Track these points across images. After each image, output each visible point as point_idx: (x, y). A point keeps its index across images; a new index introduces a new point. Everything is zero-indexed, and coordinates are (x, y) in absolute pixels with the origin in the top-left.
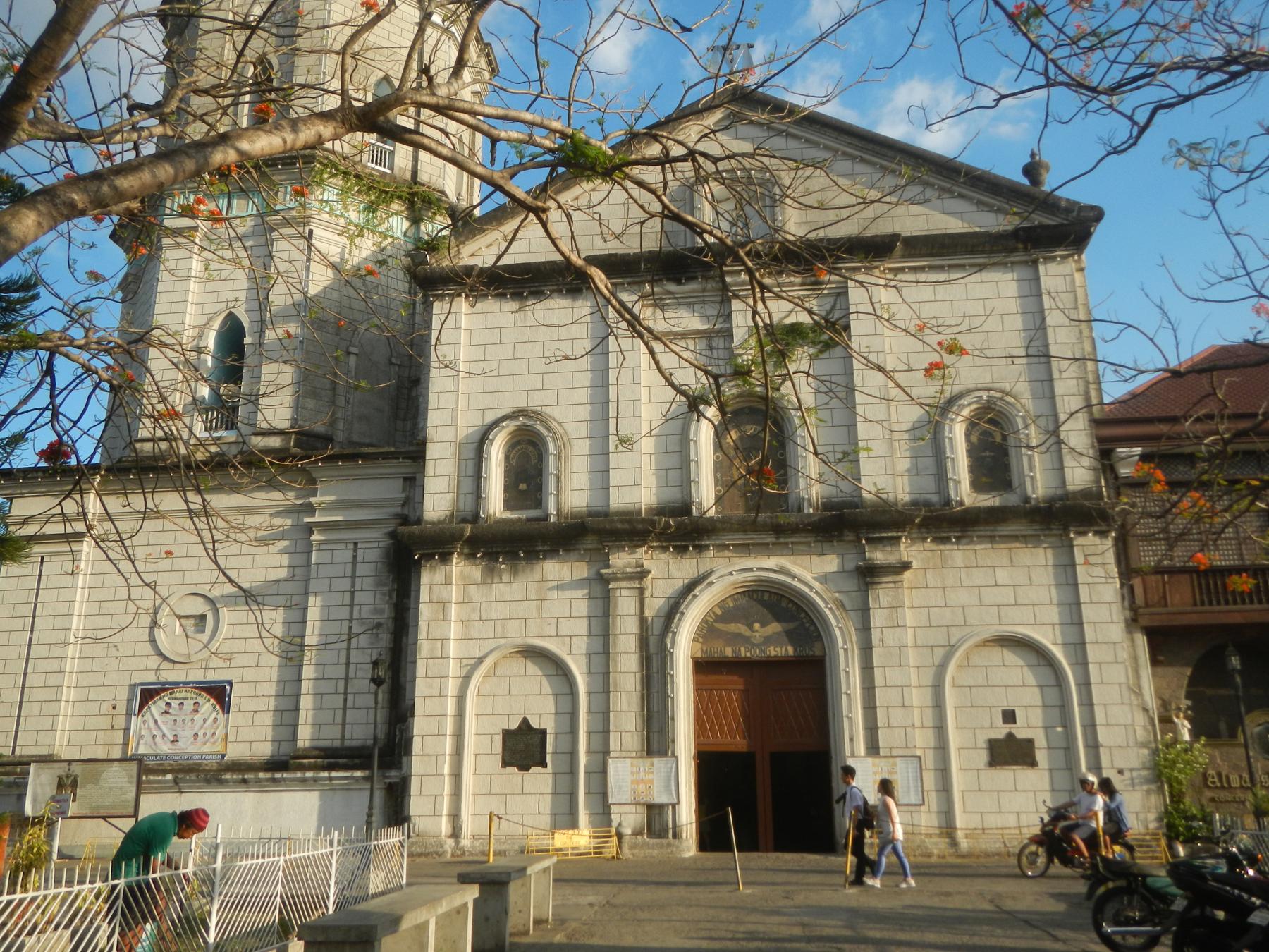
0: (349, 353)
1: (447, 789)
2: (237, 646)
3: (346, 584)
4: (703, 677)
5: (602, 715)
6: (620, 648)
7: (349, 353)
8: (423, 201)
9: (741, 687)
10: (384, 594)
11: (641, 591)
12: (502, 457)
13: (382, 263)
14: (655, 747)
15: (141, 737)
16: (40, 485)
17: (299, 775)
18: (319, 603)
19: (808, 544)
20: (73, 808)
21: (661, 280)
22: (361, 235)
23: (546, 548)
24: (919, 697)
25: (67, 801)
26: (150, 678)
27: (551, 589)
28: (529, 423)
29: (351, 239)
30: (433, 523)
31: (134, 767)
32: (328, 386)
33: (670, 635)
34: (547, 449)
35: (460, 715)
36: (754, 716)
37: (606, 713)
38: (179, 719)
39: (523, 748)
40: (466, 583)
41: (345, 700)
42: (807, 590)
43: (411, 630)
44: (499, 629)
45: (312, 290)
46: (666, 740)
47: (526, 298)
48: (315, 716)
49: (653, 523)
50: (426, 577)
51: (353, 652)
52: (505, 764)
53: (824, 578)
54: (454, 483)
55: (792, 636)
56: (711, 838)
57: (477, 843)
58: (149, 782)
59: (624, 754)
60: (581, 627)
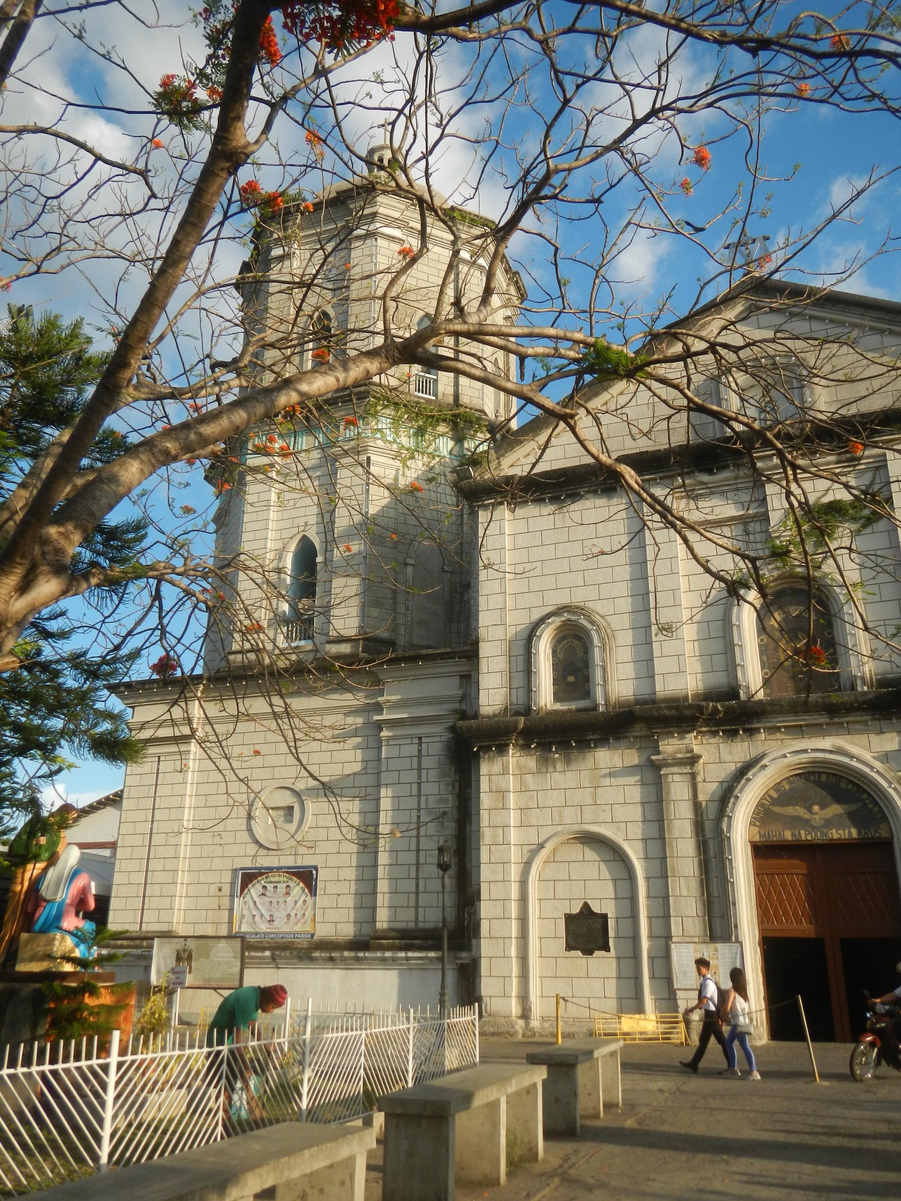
0: (406, 564)
1: (515, 971)
2: (321, 834)
3: (412, 776)
4: (763, 862)
6: (676, 833)
7: (406, 564)
8: (465, 421)
9: (805, 871)
10: (447, 785)
11: (693, 776)
12: (549, 652)
13: (430, 480)
14: (718, 933)
15: (243, 916)
16: (156, 694)
17: (379, 954)
18: (390, 795)
19: (866, 722)
20: (189, 980)
21: (693, 472)
22: (412, 458)
23: (596, 737)
25: (184, 972)
26: (248, 863)
27: (604, 776)
28: (573, 618)
29: (404, 462)
30: (489, 717)
31: (237, 943)
32: (389, 595)
33: (726, 819)
34: (592, 642)
35: (523, 899)
36: (820, 901)
37: (665, 899)
39: (586, 932)
40: (522, 773)
41: (417, 885)
42: (867, 770)
43: (474, 818)
44: (556, 816)
45: (373, 510)
46: (729, 926)
47: (563, 501)
48: (390, 899)
49: (700, 709)
50: (485, 768)
52: (569, 948)
53: (885, 757)
54: (506, 679)
56: (782, 1025)
57: (546, 1025)
58: (251, 958)
59: (687, 939)
60: (636, 813)
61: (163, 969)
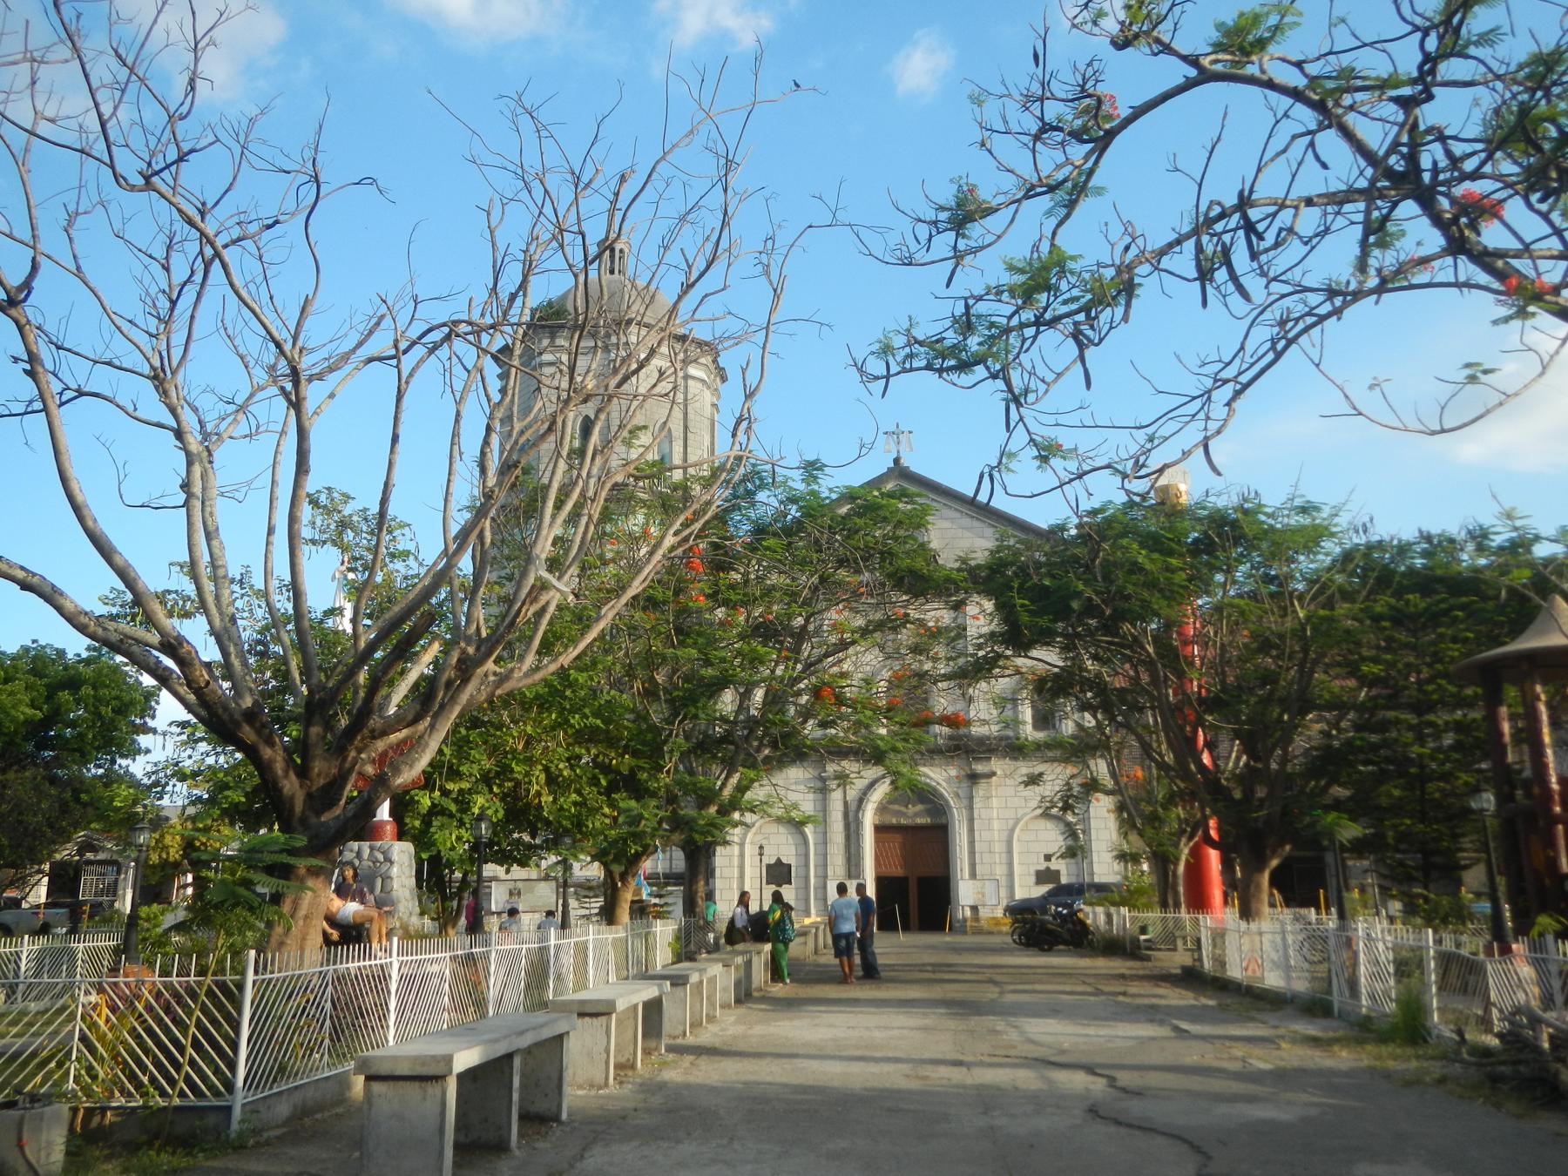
24: (999, 847)
37: (825, 855)
53: (948, 780)
55: (929, 812)
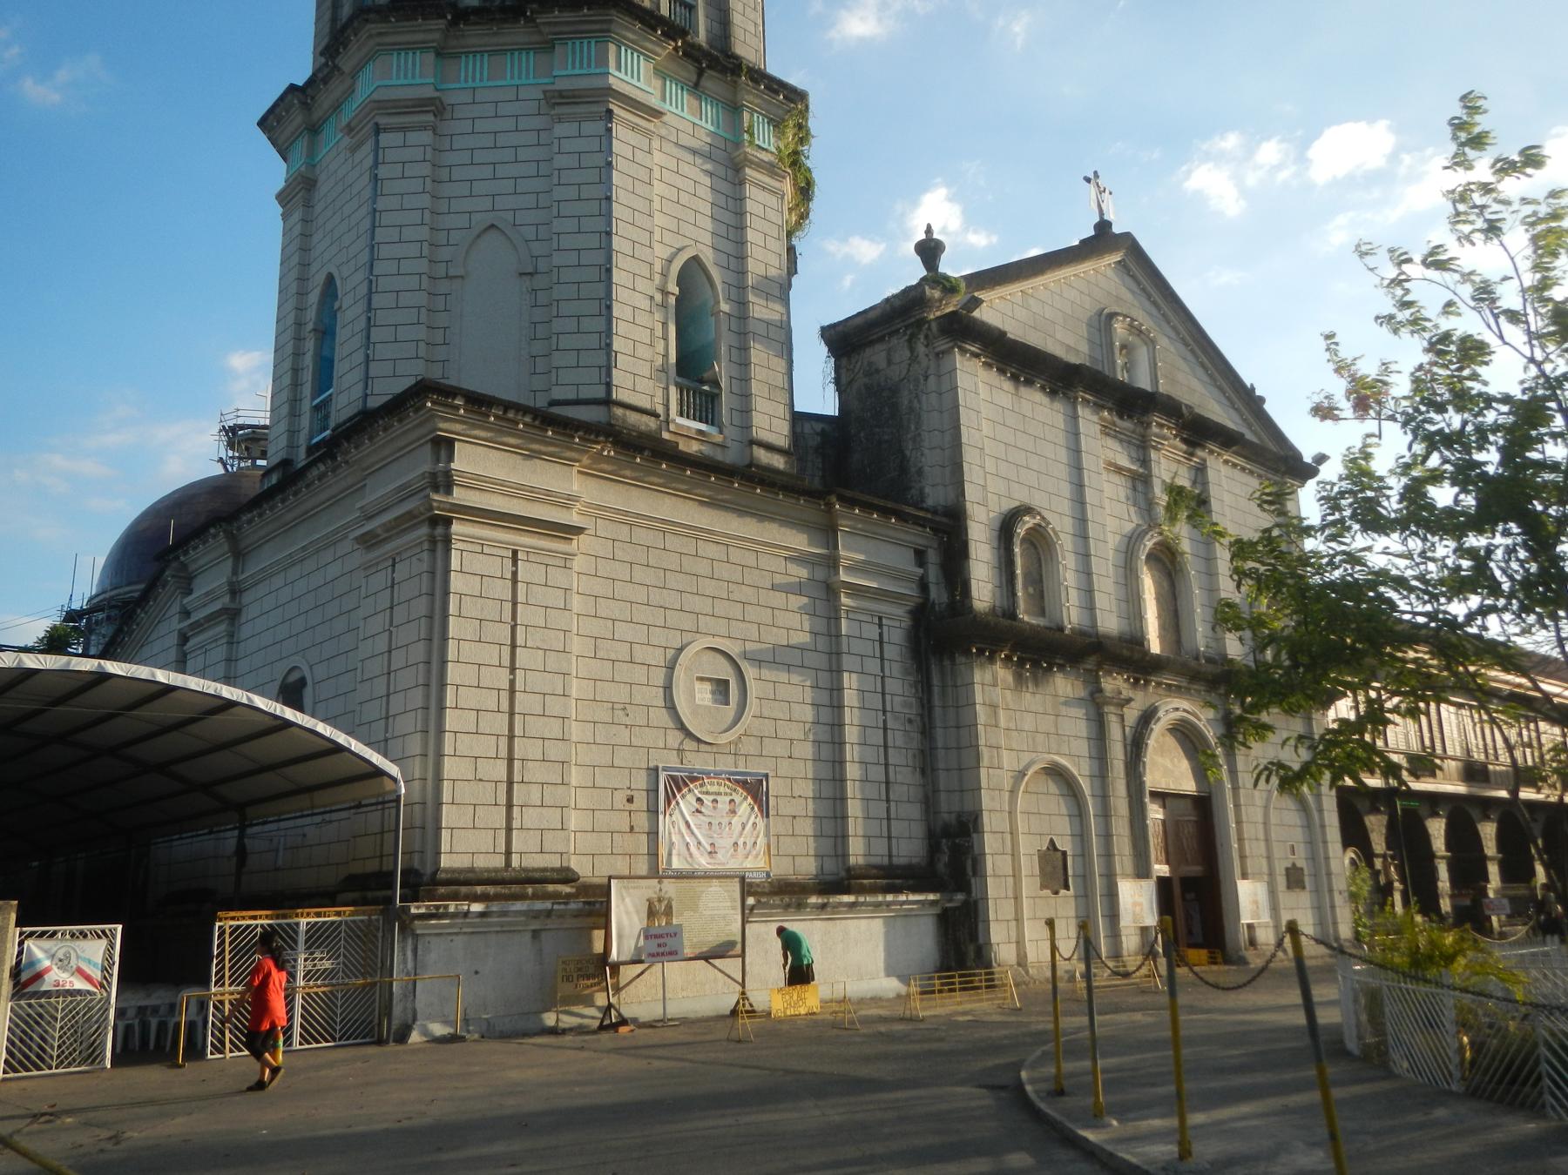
2: (767, 728)
5: (1107, 837)
11: (1122, 717)
19: (1198, 691)
31: (736, 887)
38: (715, 822)
51: (891, 751)
52: (1043, 887)
60: (1082, 747)
61: (627, 931)
